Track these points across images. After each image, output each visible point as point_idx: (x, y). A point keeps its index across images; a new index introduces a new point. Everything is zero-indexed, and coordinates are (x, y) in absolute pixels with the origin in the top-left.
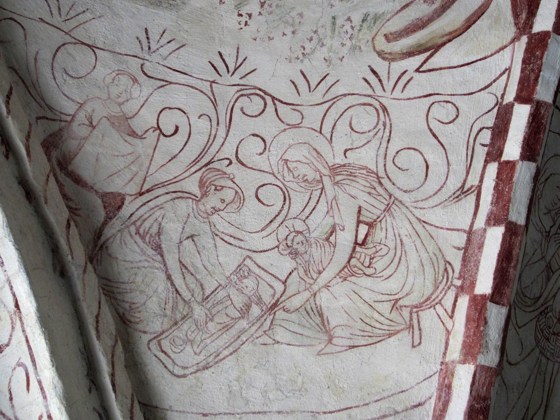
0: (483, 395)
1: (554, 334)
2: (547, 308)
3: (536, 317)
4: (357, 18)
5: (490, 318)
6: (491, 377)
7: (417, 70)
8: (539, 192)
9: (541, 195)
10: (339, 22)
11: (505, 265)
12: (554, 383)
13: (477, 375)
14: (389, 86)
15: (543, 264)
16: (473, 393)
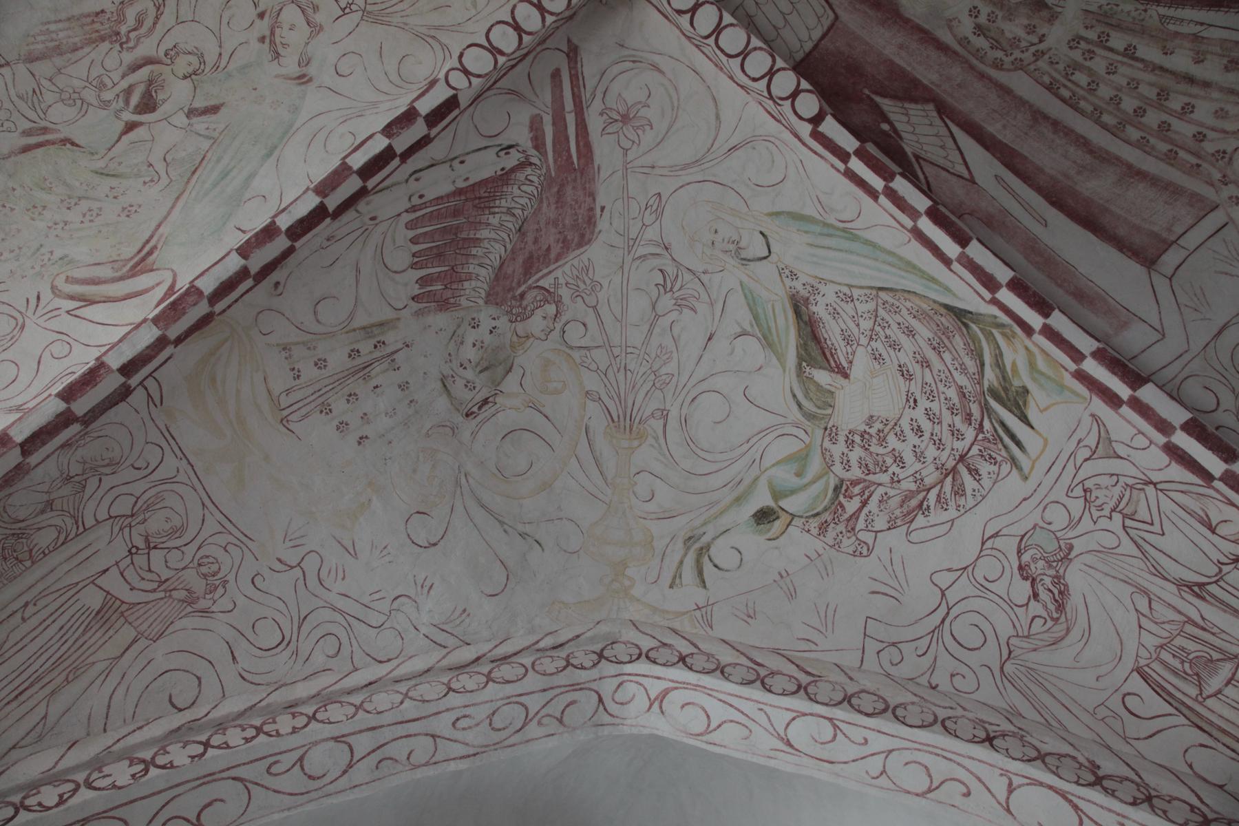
1: (17, 559)
4: (58, 253)
7: (68, 312)
10: (43, 250)
14: (40, 312)
15: (45, 497)
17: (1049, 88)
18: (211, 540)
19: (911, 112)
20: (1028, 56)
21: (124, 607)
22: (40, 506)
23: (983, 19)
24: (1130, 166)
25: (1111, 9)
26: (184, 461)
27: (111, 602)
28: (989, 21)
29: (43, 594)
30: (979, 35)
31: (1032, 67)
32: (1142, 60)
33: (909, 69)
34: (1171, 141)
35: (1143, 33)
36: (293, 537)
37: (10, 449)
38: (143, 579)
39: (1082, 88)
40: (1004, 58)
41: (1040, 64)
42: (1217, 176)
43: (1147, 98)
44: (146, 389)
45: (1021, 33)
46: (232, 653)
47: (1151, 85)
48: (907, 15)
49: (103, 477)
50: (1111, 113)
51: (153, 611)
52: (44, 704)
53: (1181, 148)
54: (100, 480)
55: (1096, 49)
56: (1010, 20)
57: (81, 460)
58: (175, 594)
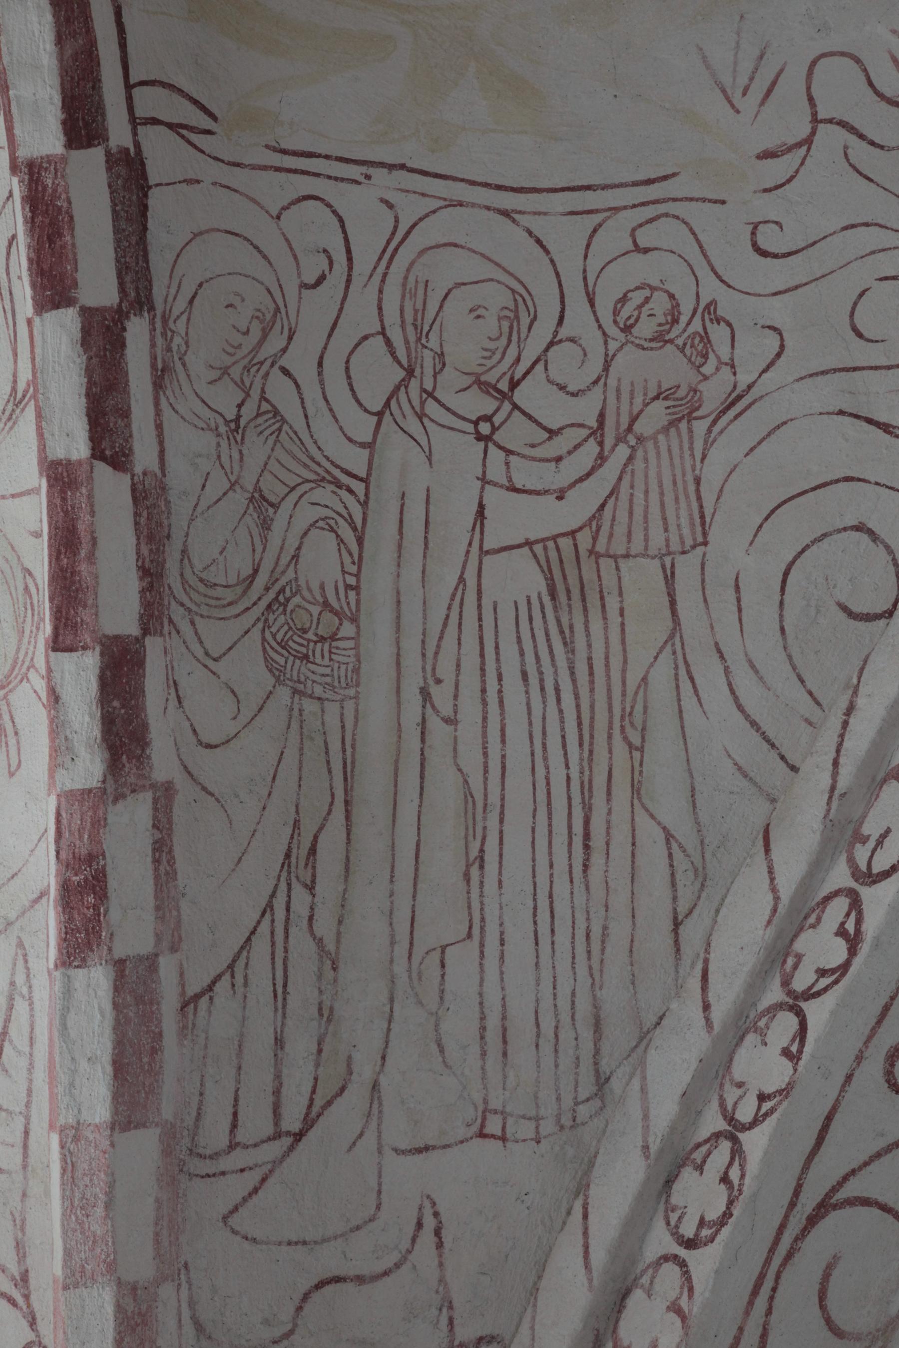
0: (84, 852)
1: (322, 639)
2: (282, 590)
3: (258, 619)
5: (62, 686)
6: (95, 808)
8: (177, 340)
9: (187, 343)
11: (65, 561)
12: (353, 747)
13: (64, 814)
15: (239, 498)
16: (63, 855)
18: (594, 265)
21: (584, 539)
22: (251, 521)
26: (379, 174)
27: (553, 554)
29: (430, 654)
36: (743, 80)
37: (90, 479)
38: (559, 459)
44: (155, 121)
46: (870, 421)
49: (283, 362)
51: (639, 496)
52: (642, 818)
54: (285, 372)
57: (215, 374)
58: (642, 427)
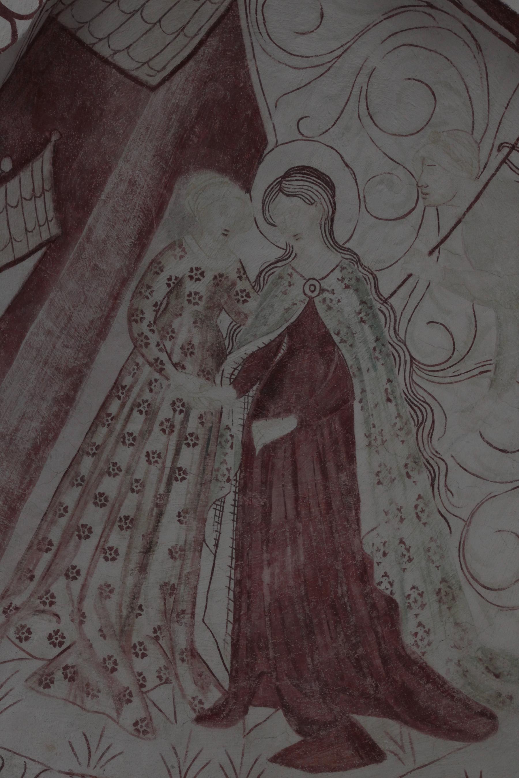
17: (117, 386)
19: (40, 203)
20: (153, 352)
23: (190, 286)
24: (22, 498)
25: (227, 441)
28: (190, 295)
30: (169, 285)
31: (140, 360)
32: (168, 491)
33: (103, 197)
34: (64, 542)
35: (201, 484)
39: (124, 426)
40: (145, 323)
41: (147, 369)
42: (17, 601)
43: (121, 505)
45: (182, 338)
47: (139, 508)
48: (176, 186)
50: (95, 466)
53: (55, 555)
55: (175, 433)
56: (195, 322)
